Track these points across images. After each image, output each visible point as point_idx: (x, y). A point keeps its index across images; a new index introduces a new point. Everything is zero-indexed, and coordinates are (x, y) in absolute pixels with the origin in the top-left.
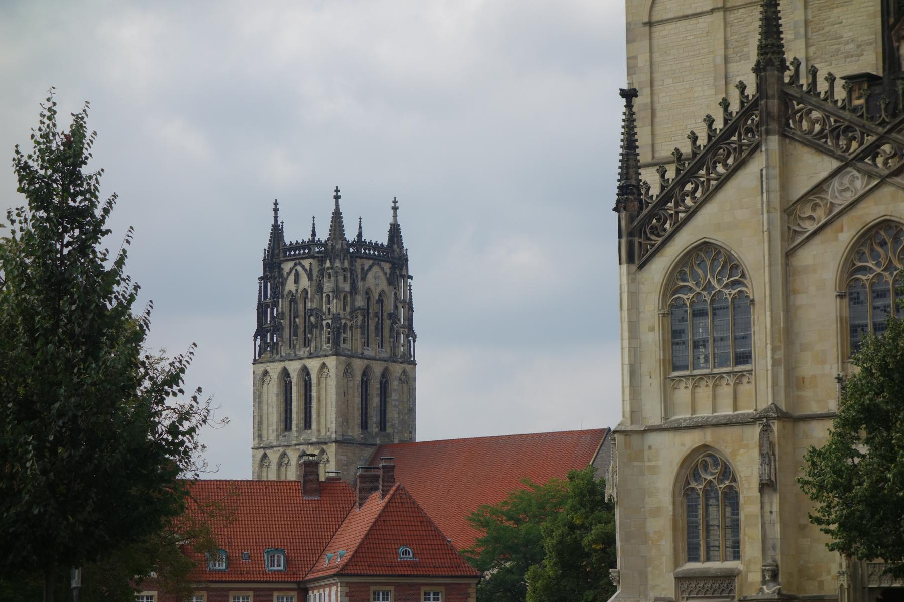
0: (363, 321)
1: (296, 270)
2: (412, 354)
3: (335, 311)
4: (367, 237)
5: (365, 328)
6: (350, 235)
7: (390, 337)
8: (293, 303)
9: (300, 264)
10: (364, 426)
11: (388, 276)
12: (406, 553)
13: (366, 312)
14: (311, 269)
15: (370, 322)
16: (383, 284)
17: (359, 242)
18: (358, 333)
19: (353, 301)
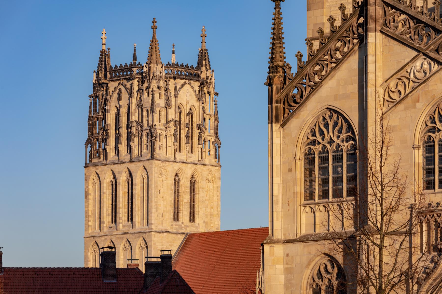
0: (176, 131)
7: (199, 144)
10: (176, 218)
16: (193, 101)
18: (171, 141)
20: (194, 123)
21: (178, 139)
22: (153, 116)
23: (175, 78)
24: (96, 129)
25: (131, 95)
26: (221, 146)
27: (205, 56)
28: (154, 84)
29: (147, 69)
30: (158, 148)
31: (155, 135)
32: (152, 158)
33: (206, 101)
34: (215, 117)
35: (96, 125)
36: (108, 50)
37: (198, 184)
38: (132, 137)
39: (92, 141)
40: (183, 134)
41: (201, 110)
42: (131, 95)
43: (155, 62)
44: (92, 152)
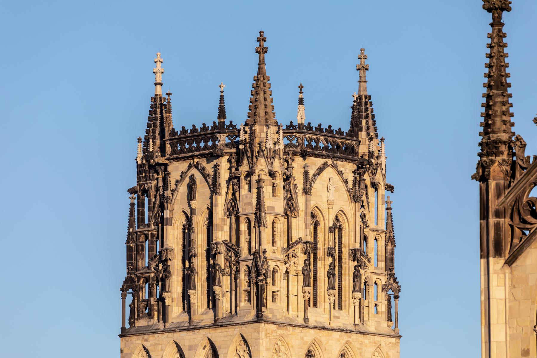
0: (307, 263)
7: (354, 290)
20: (345, 247)
21: (312, 280)
22: (260, 232)
23: (304, 155)
24: (143, 258)
25: (214, 189)
26: (400, 294)
27: (367, 110)
28: (261, 165)
29: (247, 136)
30: (270, 299)
31: (264, 272)
32: (259, 318)
33: (368, 203)
34: (388, 235)
35: (143, 249)
36: (166, 97)
38: (218, 276)
39: (135, 282)
40: (323, 270)
41: (359, 220)
42: (214, 189)
43: (263, 121)
44: (136, 306)
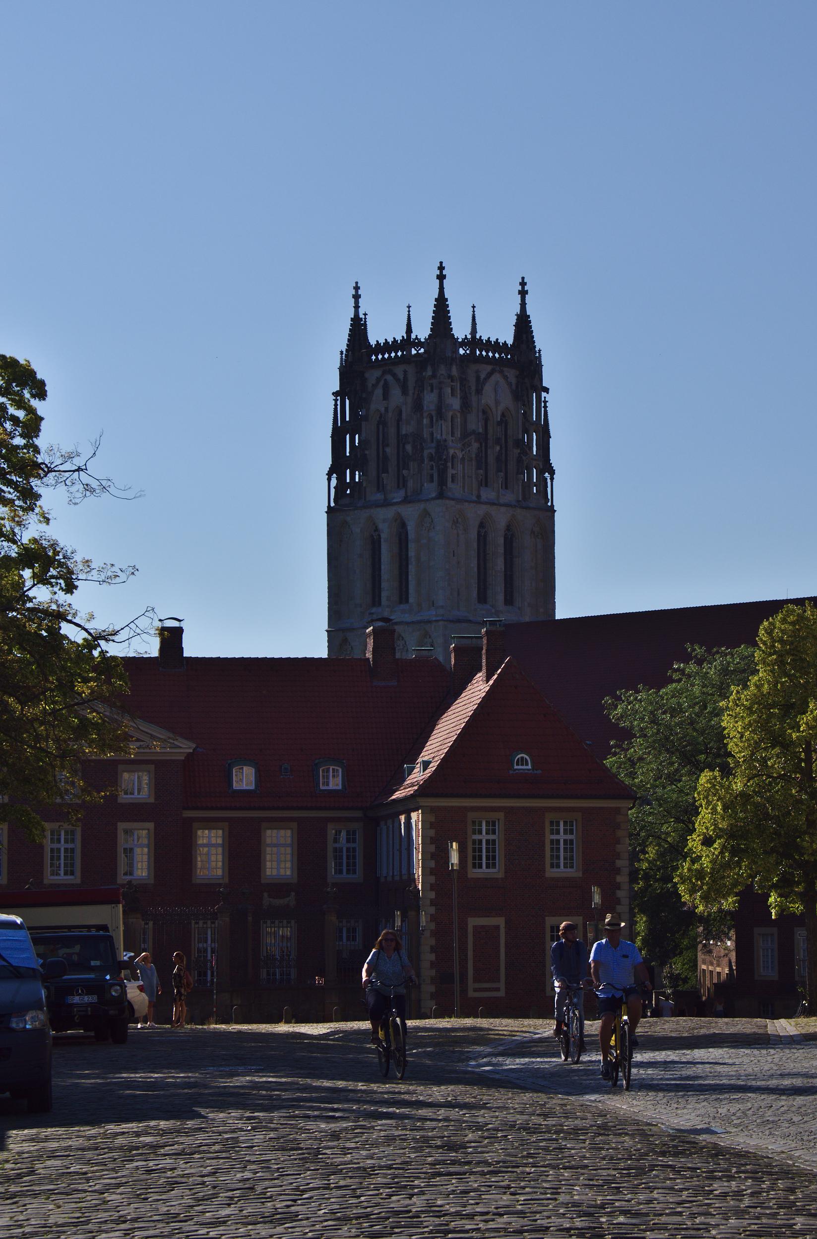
1: (386, 380)
2: (549, 497)
3: (439, 437)
4: (483, 333)
5: (481, 461)
6: (460, 330)
8: (381, 427)
9: (391, 372)
10: (482, 598)
11: (514, 387)
12: (522, 761)
13: (483, 439)
14: (405, 378)
15: (489, 451)
16: (506, 400)
17: (474, 342)
19: (465, 422)
30: (450, 480)
32: (441, 496)
37: (517, 541)
